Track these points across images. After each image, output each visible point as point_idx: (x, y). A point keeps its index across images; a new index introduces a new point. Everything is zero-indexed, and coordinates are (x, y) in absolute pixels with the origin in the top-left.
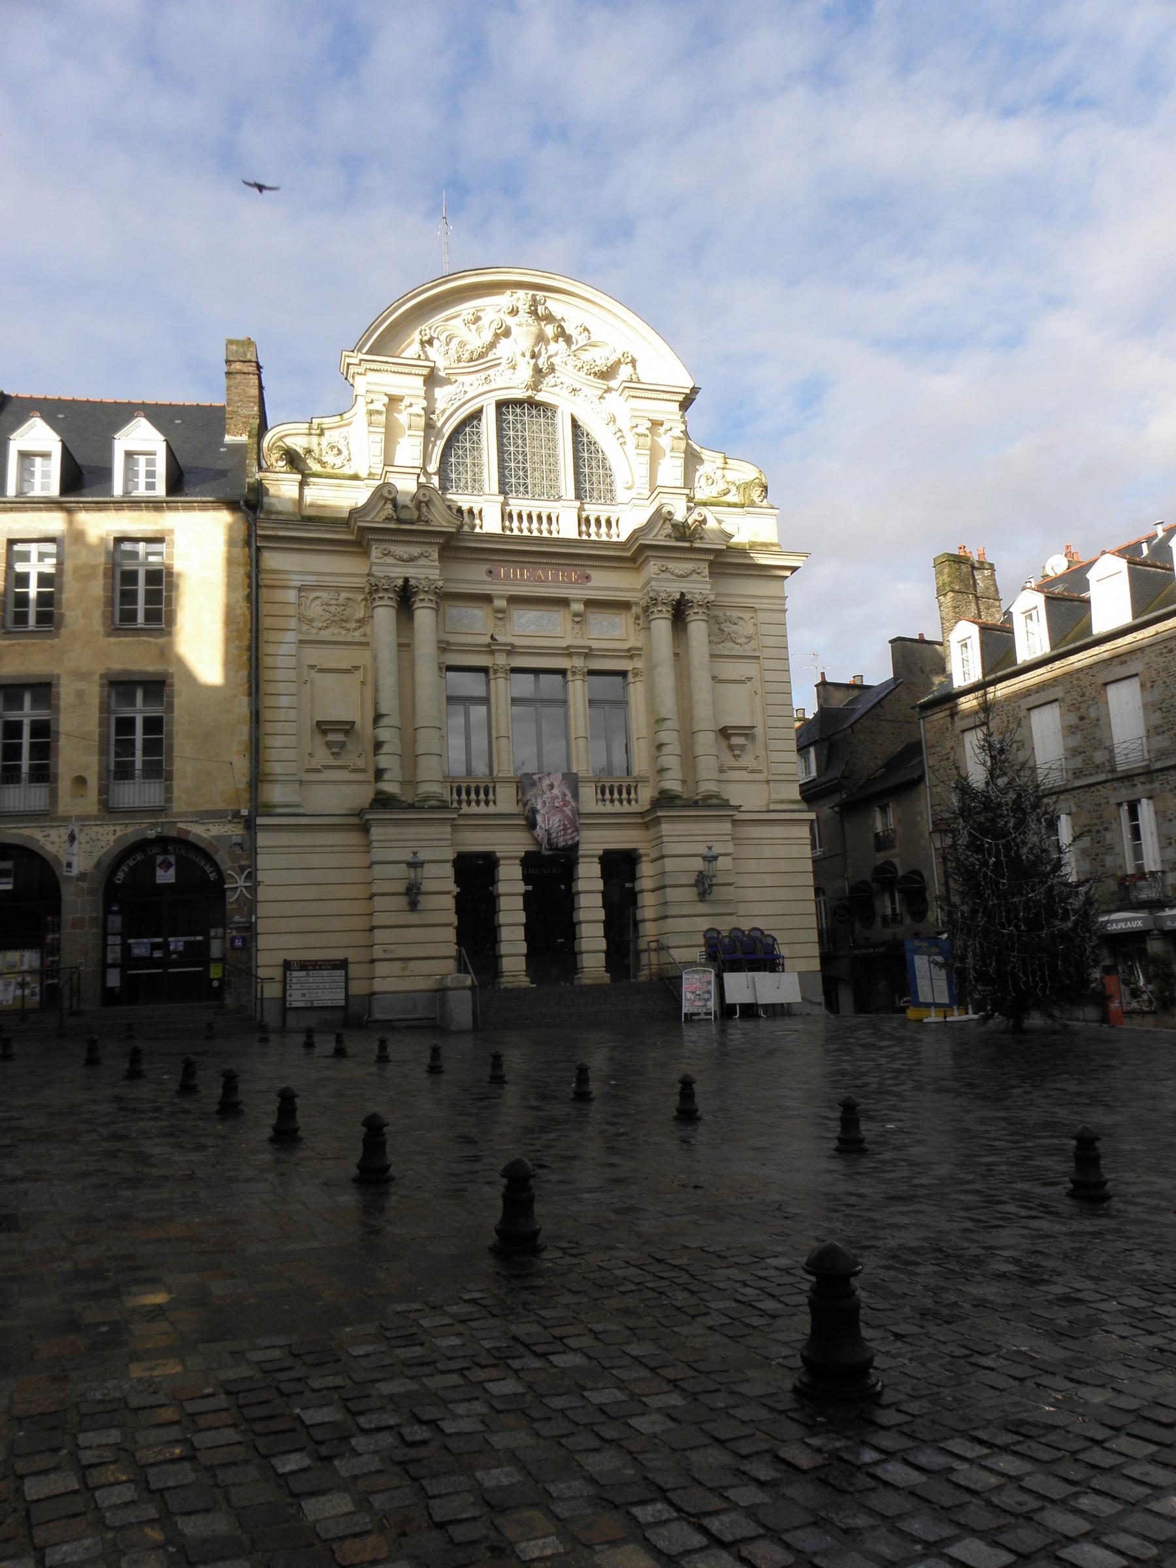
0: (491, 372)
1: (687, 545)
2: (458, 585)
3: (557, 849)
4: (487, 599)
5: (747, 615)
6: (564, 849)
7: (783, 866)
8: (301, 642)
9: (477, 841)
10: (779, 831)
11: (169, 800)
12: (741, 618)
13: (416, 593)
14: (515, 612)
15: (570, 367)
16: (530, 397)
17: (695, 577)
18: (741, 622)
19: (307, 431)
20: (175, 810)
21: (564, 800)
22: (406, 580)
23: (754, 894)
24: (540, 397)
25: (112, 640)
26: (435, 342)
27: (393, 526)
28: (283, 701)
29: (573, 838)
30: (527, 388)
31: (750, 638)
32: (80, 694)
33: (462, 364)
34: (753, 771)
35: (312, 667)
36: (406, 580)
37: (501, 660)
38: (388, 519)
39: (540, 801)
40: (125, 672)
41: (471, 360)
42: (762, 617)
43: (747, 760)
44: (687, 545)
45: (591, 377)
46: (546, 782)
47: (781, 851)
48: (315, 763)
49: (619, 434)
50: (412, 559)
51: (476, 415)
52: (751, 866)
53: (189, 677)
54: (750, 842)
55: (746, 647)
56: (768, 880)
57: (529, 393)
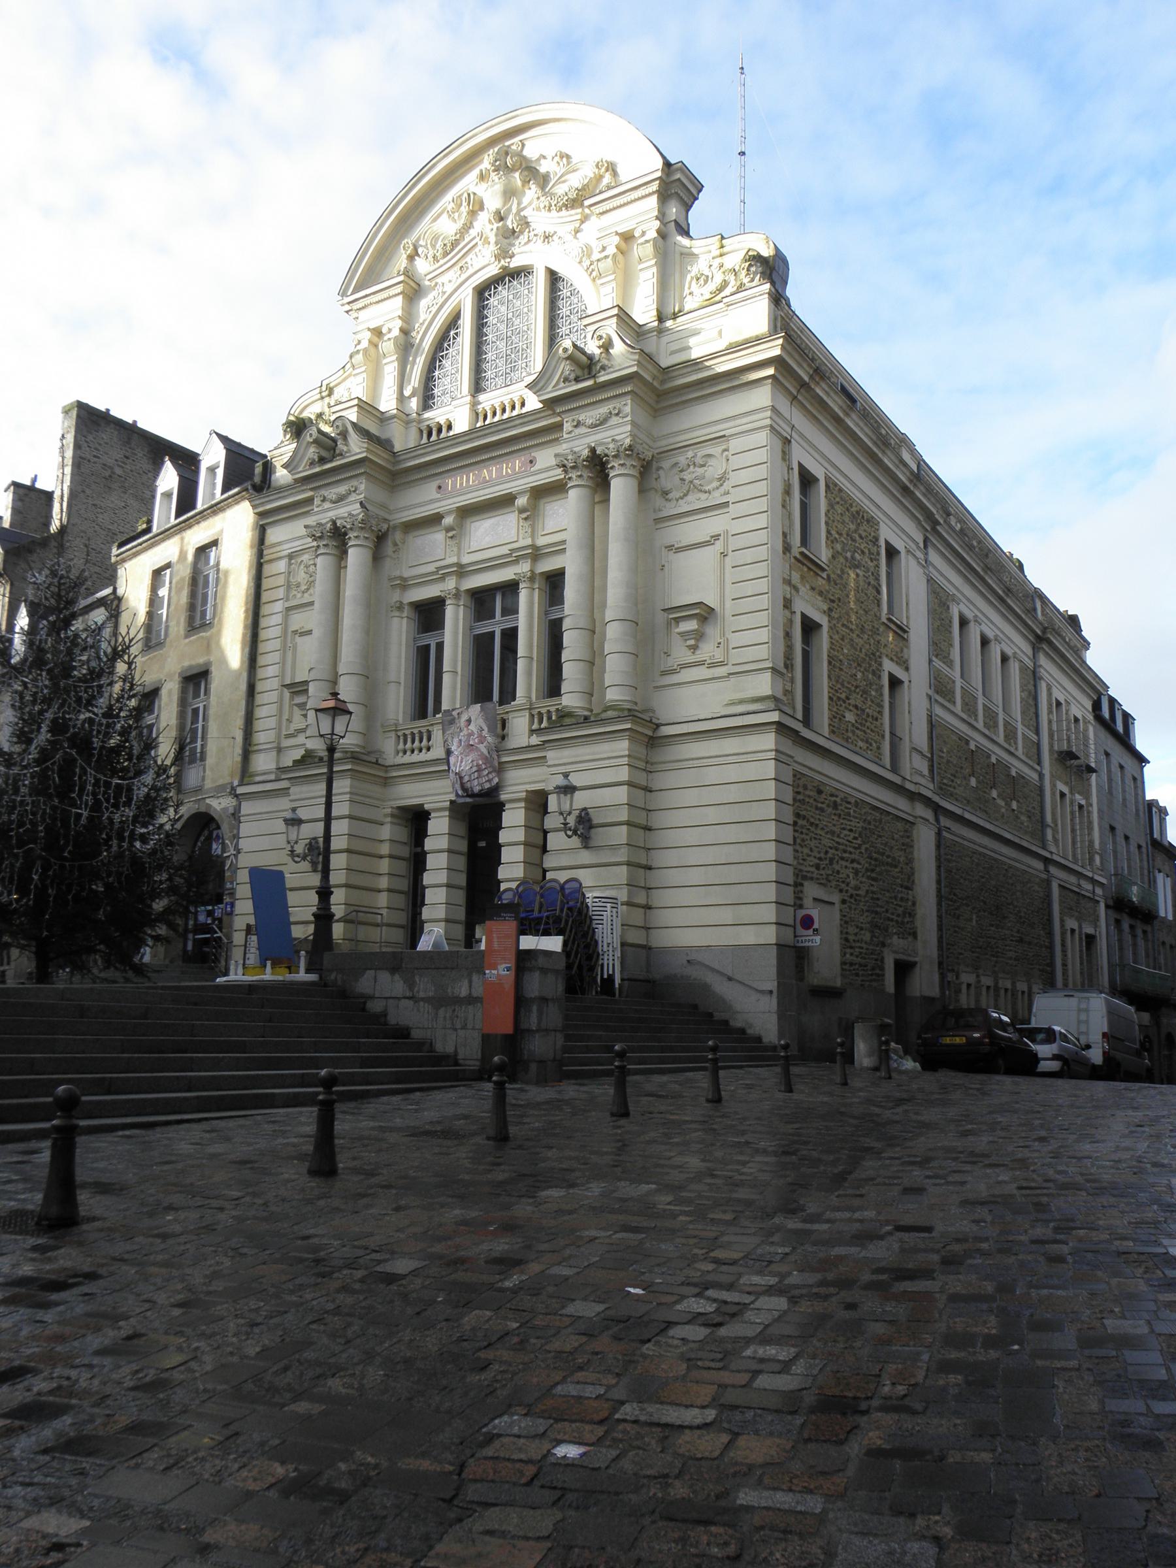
0: (468, 259)
1: (590, 383)
3: (473, 795)
4: (434, 520)
5: (716, 450)
6: (481, 794)
7: (733, 794)
8: (288, 609)
9: (411, 793)
10: (730, 745)
11: (203, 779)
12: (709, 456)
17: (615, 420)
18: (712, 462)
19: (318, 396)
20: (206, 787)
21: (480, 736)
22: (334, 523)
23: (692, 836)
24: (515, 263)
25: (187, 640)
27: (317, 469)
28: (269, 672)
29: (489, 781)
30: (498, 257)
31: (722, 479)
32: (170, 691)
33: (442, 262)
34: (713, 665)
35: (295, 632)
36: (334, 523)
37: (451, 584)
38: (312, 464)
39: (456, 740)
40: (191, 667)
41: (446, 254)
42: (735, 445)
43: (708, 650)
44: (590, 383)
45: (564, 212)
46: (464, 717)
47: (732, 773)
48: (294, 726)
52: (691, 797)
53: (223, 661)
54: (677, 765)
55: (716, 494)
56: (712, 815)
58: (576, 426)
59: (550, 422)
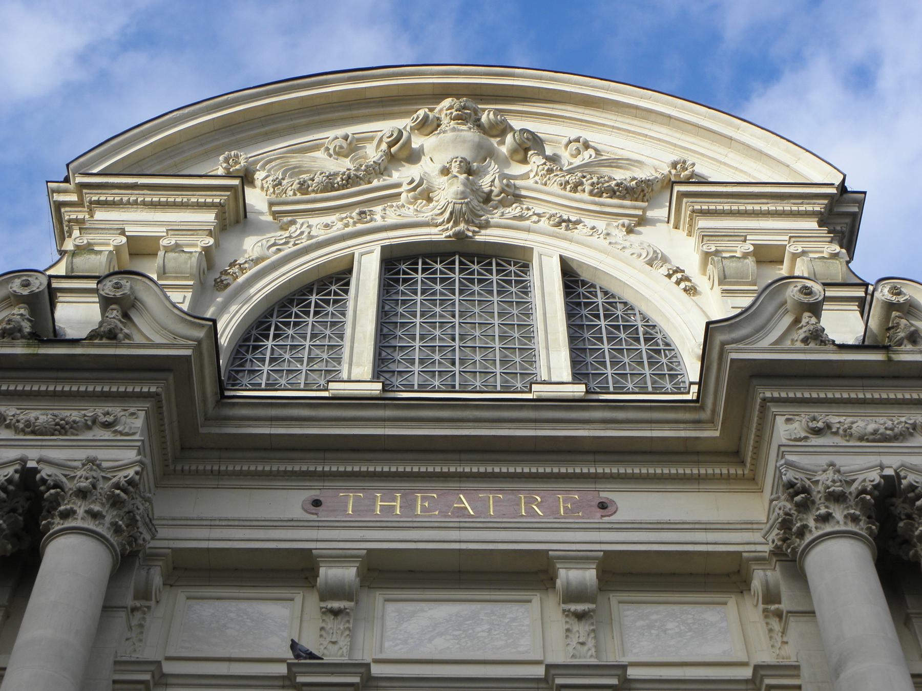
2: (217, 533)
13: (55, 502)
14: (391, 608)
15: (556, 188)
16: (460, 236)
26: (259, 176)
49: (679, 275)
50: (61, 428)
51: (339, 277)
57: (462, 226)
58: (817, 432)
59: (683, 434)
